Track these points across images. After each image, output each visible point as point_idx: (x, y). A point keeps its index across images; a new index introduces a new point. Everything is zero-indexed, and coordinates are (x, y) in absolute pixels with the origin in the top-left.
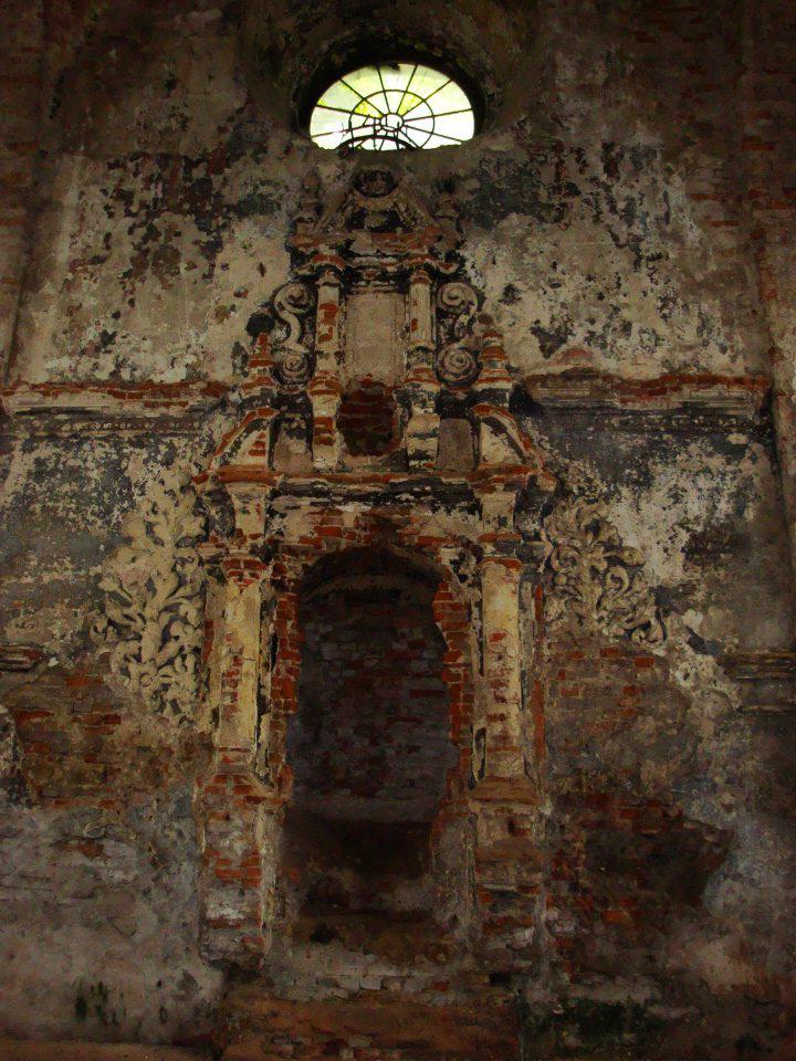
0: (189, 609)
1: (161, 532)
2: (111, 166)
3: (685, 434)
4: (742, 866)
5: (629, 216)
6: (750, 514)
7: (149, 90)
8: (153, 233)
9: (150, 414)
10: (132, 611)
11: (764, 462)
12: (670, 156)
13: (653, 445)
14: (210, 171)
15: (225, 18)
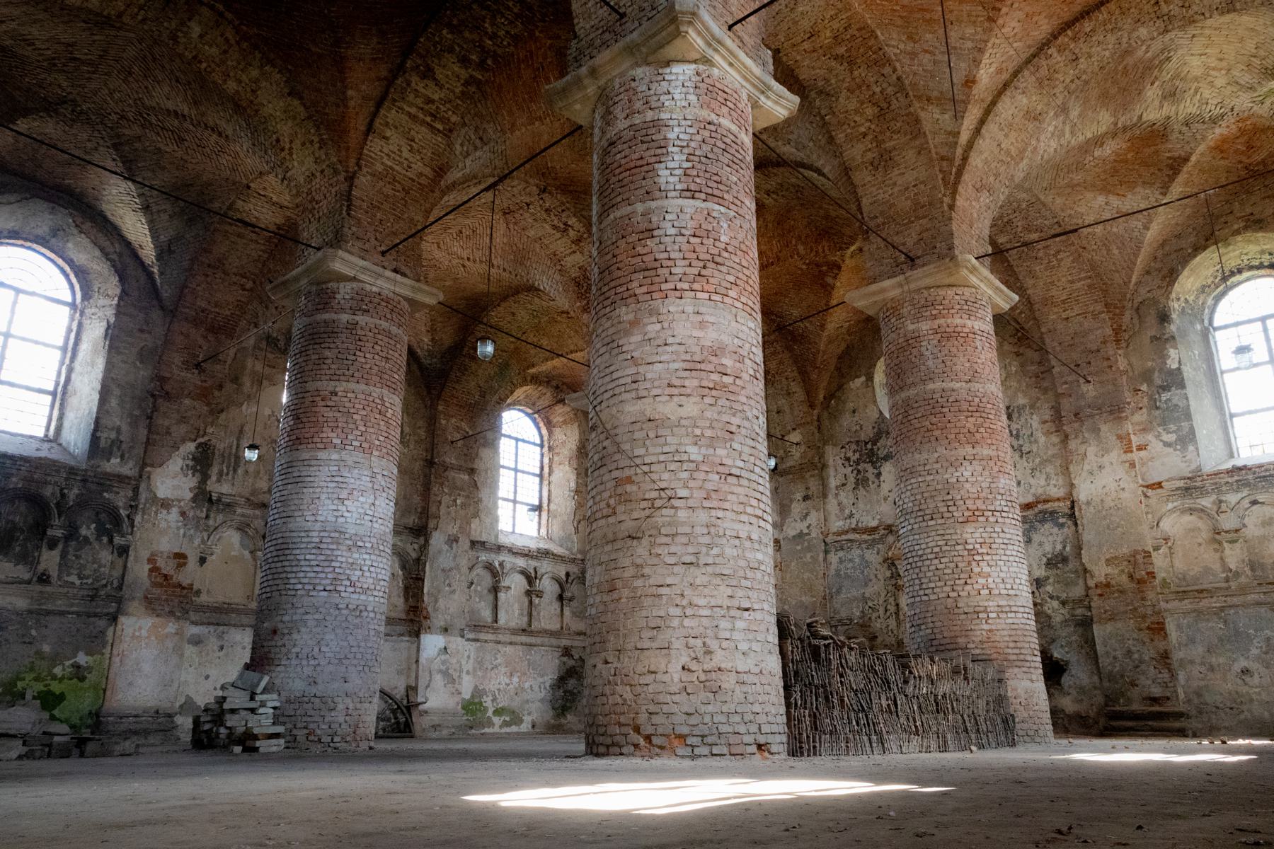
0: (891, 600)
1: (879, 576)
2: (842, 448)
3: (1043, 521)
4: (1073, 672)
5: (1017, 437)
6: (1068, 549)
7: (847, 416)
8: (859, 472)
9: (869, 537)
10: (875, 603)
11: (1073, 528)
12: (1032, 407)
13: (1031, 527)
14: (873, 445)
15: (867, 380)
